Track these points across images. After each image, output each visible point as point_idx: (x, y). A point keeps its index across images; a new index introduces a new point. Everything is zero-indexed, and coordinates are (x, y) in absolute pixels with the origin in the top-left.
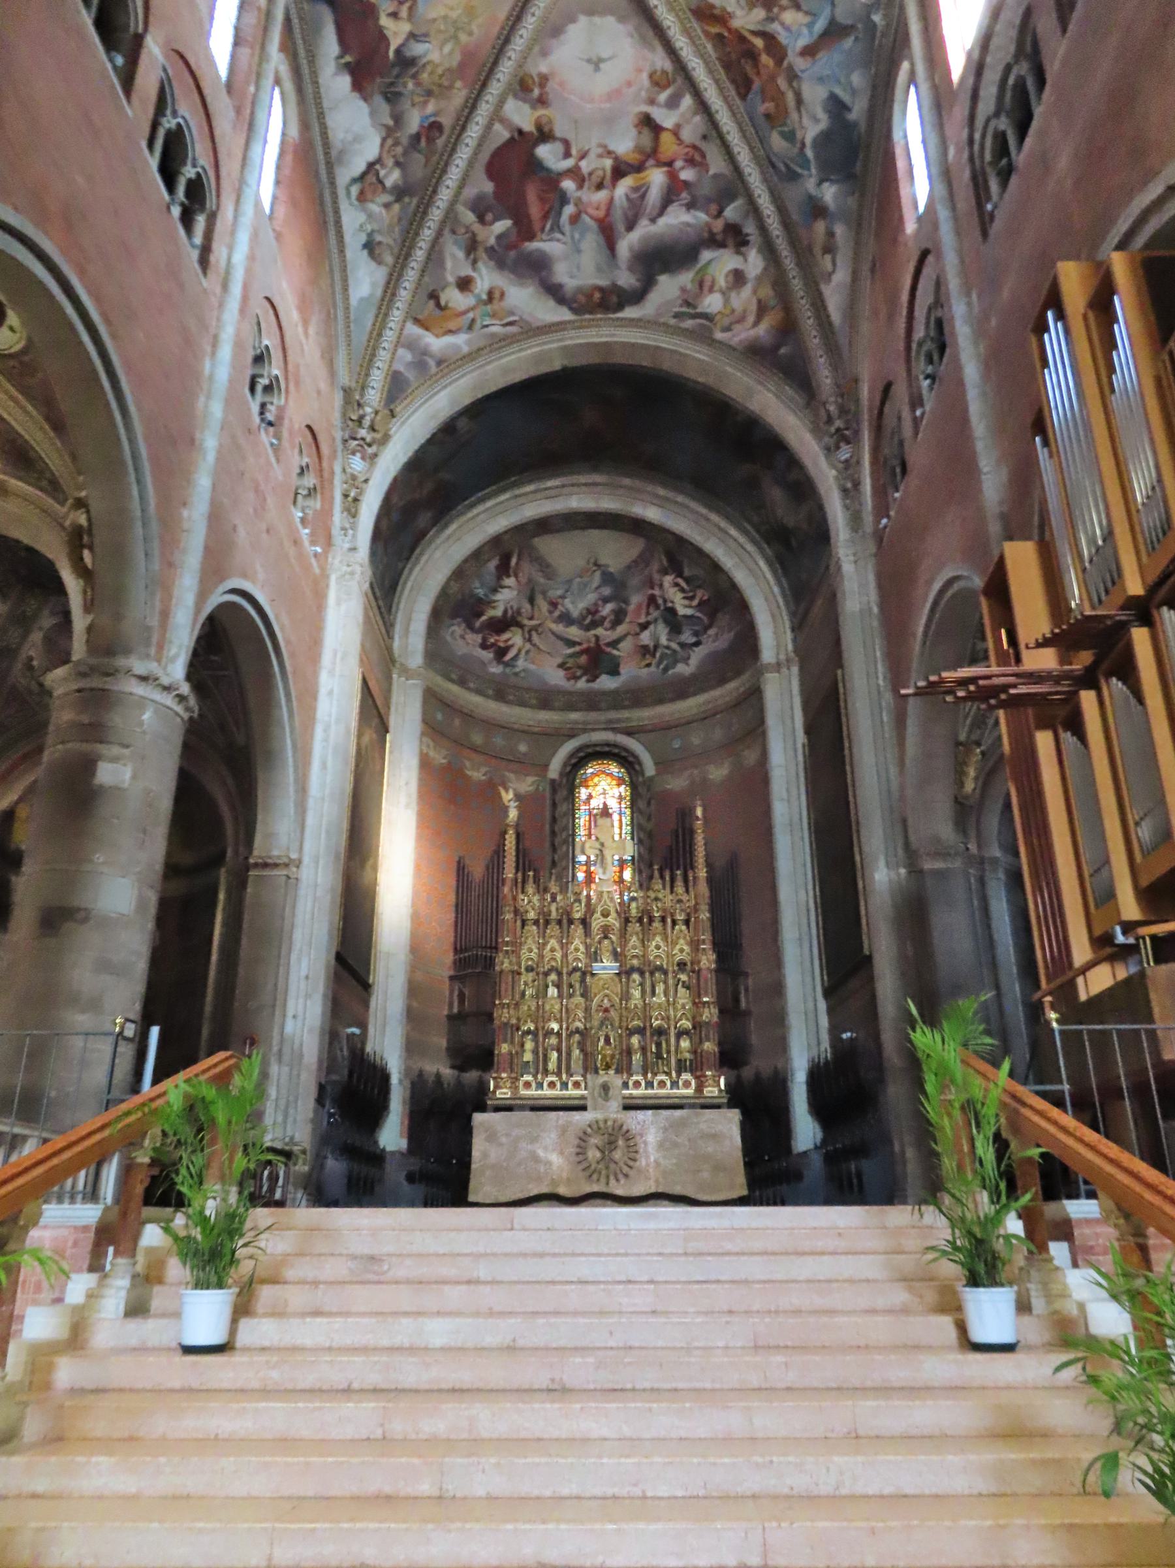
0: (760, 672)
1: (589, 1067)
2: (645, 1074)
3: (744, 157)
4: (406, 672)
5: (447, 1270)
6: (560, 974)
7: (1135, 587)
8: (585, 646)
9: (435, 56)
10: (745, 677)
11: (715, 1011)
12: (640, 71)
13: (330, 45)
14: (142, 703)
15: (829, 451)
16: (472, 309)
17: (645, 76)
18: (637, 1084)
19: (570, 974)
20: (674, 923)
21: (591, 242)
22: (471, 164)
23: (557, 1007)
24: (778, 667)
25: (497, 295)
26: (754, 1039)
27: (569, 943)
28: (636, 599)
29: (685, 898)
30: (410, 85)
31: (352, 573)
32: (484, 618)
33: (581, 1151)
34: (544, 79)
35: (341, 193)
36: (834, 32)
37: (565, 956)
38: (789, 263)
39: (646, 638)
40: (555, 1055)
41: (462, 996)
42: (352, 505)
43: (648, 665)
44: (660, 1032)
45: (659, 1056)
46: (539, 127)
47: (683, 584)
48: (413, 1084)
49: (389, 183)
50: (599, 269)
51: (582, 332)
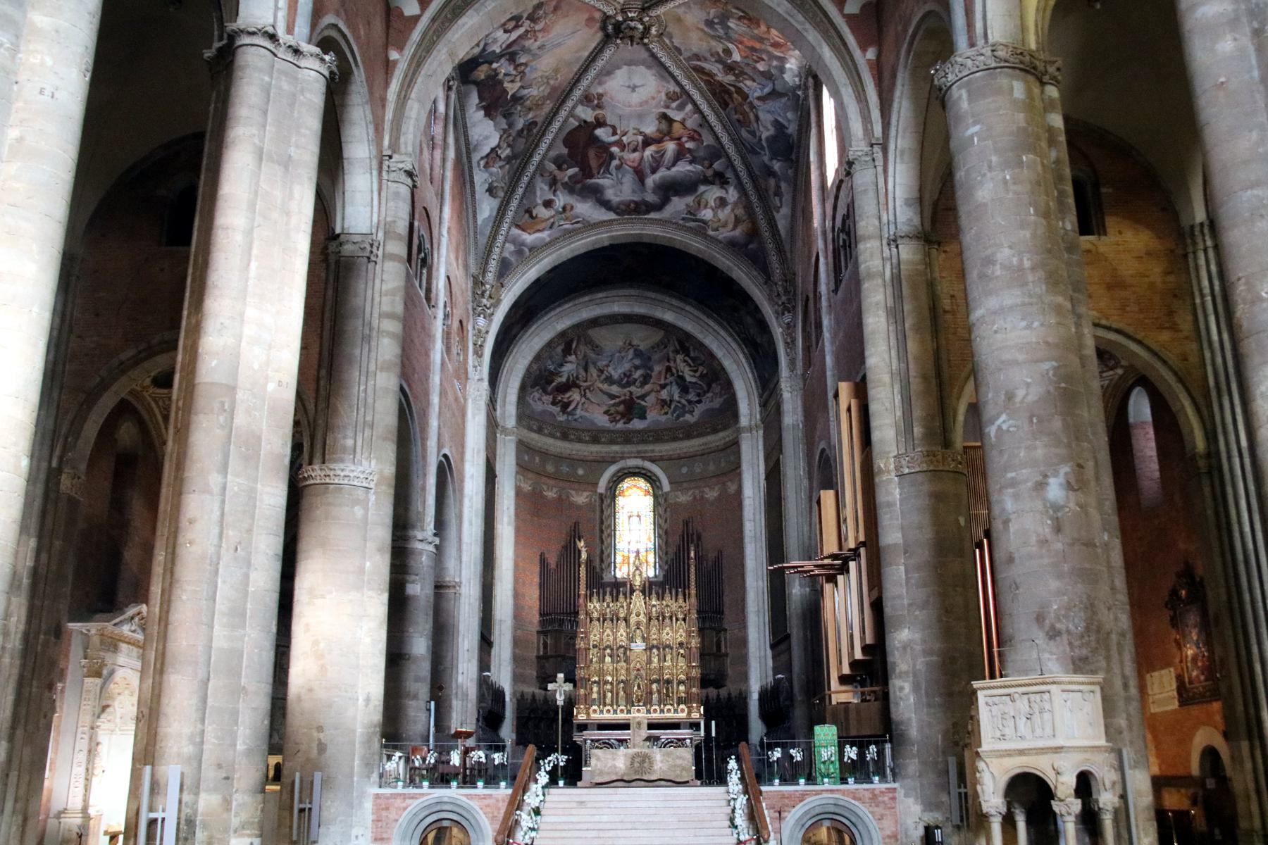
0: (739, 431)
1: (630, 702)
2: (659, 705)
3: (725, 139)
4: (505, 431)
5: (602, 805)
6: (612, 649)
7: (852, 544)
8: (623, 398)
11: (699, 671)
12: (660, 92)
13: (474, 99)
14: (421, 553)
15: (779, 315)
16: (553, 217)
18: (655, 711)
19: (618, 649)
20: (677, 620)
21: (628, 181)
22: (554, 140)
23: (611, 668)
24: (750, 429)
25: (568, 208)
26: (730, 671)
28: (657, 368)
29: (684, 605)
30: (519, 108)
31: (480, 396)
33: (632, 763)
34: (600, 96)
35: (474, 164)
36: (774, 94)
37: (615, 639)
38: (754, 198)
39: (664, 394)
40: (609, 695)
42: (478, 353)
43: (666, 413)
44: (668, 682)
45: (668, 695)
46: (596, 118)
47: (690, 361)
48: (518, 700)
50: (634, 191)
51: (622, 227)
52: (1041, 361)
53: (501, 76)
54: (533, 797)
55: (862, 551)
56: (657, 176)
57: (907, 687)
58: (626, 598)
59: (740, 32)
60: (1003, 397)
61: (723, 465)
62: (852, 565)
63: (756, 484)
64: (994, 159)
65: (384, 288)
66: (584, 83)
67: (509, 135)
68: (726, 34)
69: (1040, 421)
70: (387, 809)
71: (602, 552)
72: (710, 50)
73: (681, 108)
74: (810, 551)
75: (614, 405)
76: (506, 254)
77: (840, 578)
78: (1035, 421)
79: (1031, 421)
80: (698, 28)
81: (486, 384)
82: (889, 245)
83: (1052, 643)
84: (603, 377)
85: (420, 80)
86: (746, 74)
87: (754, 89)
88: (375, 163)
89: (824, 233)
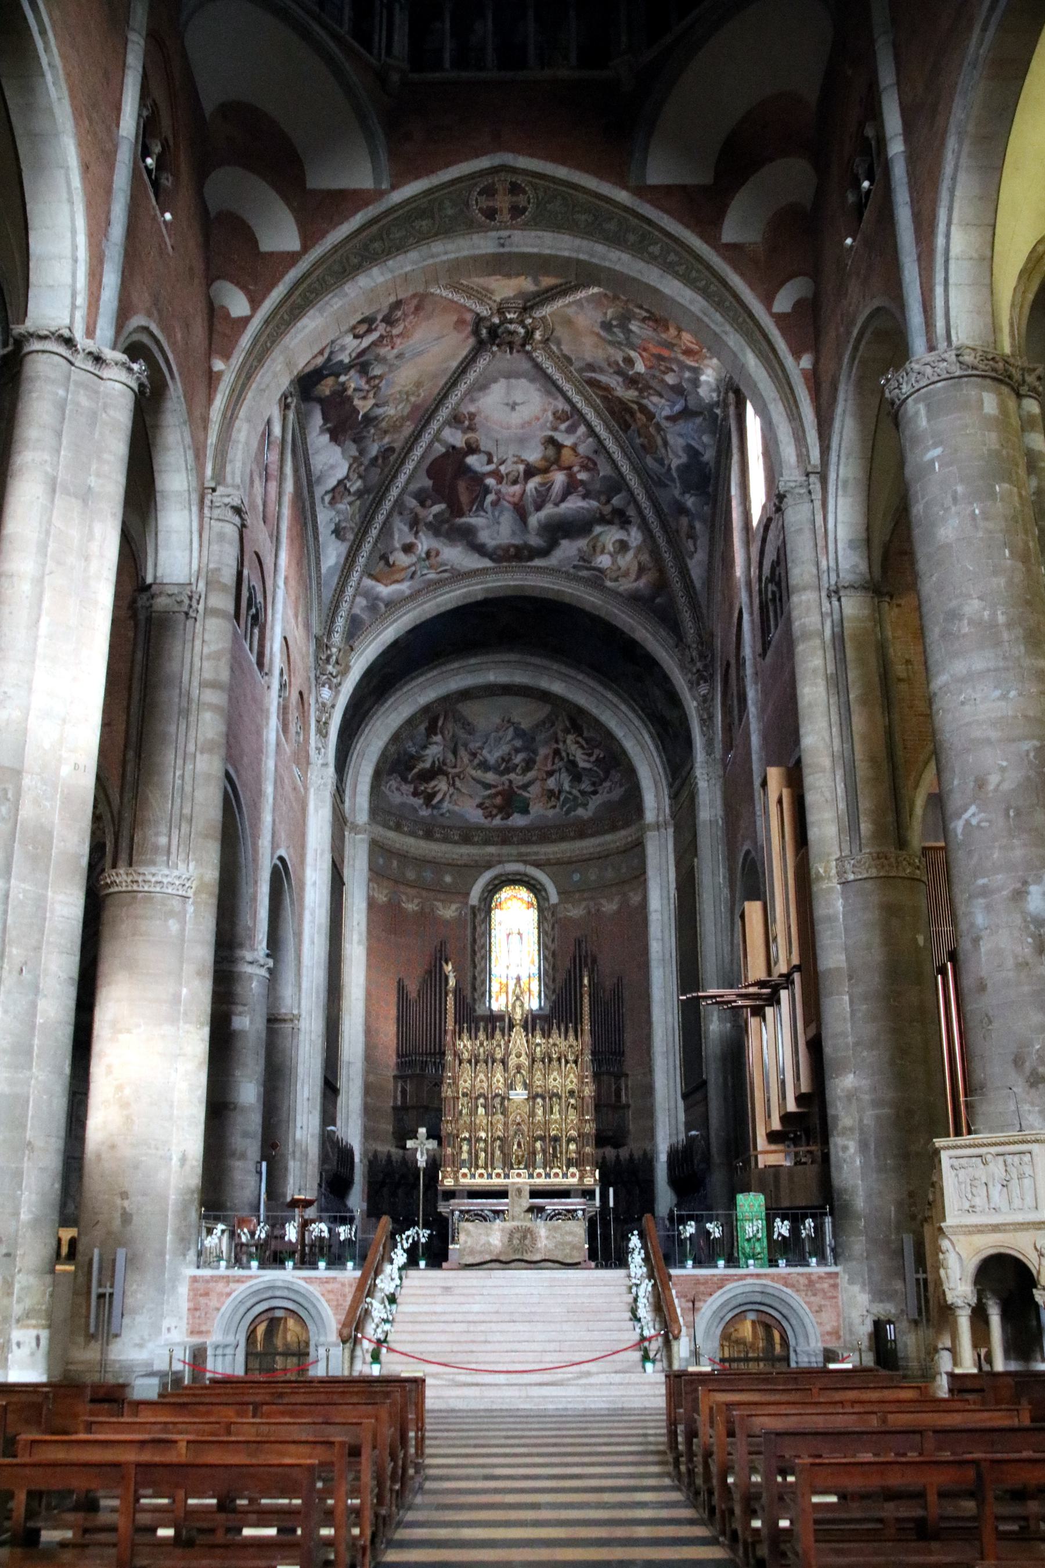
0: (643, 829)
2: (544, 1168)
3: (625, 468)
4: (355, 829)
5: (473, 1291)
6: (486, 1099)
7: (782, 968)
8: (500, 788)
9: (392, 412)
10: (631, 830)
11: (593, 1125)
12: (545, 410)
13: (317, 420)
14: (251, 977)
15: (693, 685)
16: (414, 564)
17: (550, 414)
18: (539, 1175)
19: (493, 1098)
20: (567, 1062)
22: (415, 469)
24: (658, 826)
25: (433, 553)
26: (631, 1127)
27: (493, 1076)
28: (543, 751)
29: (575, 1043)
30: (372, 431)
31: (325, 785)
32: (416, 770)
33: (510, 1240)
34: (472, 416)
35: (318, 501)
36: (686, 413)
37: (490, 1086)
38: (662, 542)
39: (551, 783)
40: (483, 1155)
41: (404, 1092)
42: (323, 732)
43: (554, 807)
44: (556, 1139)
45: (555, 1156)
46: (468, 443)
47: (583, 743)
48: (370, 1162)
49: (352, 490)
50: (514, 533)
52: (1019, 739)
53: (350, 392)
54: (386, 1284)
55: (797, 977)
56: (542, 514)
57: (852, 1146)
58: (503, 1035)
59: (644, 336)
60: (972, 784)
61: (624, 870)
62: (784, 994)
63: (665, 895)
64: (960, 489)
65: (206, 650)
66: (453, 400)
67: (361, 464)
68: (627, 339)
69: (1018, 814)
70: (206, 1294)
71: (474, 978)
72: (607, 359)
73: (572, 430)
74: (732, 977)
75: (489, 797)
76: (357, 611)
77: (769, 1011)
78: (1012, 814)
79: (1007, 815)
80: (593, 332)
81: (331, 770)
82: (829, 597)
83: (1033, 1090)
84: (476, 761)
85: (250, 395)
86: (651, 388)
87: (661, 407)
88: (195, 497)
89: (749, 584)
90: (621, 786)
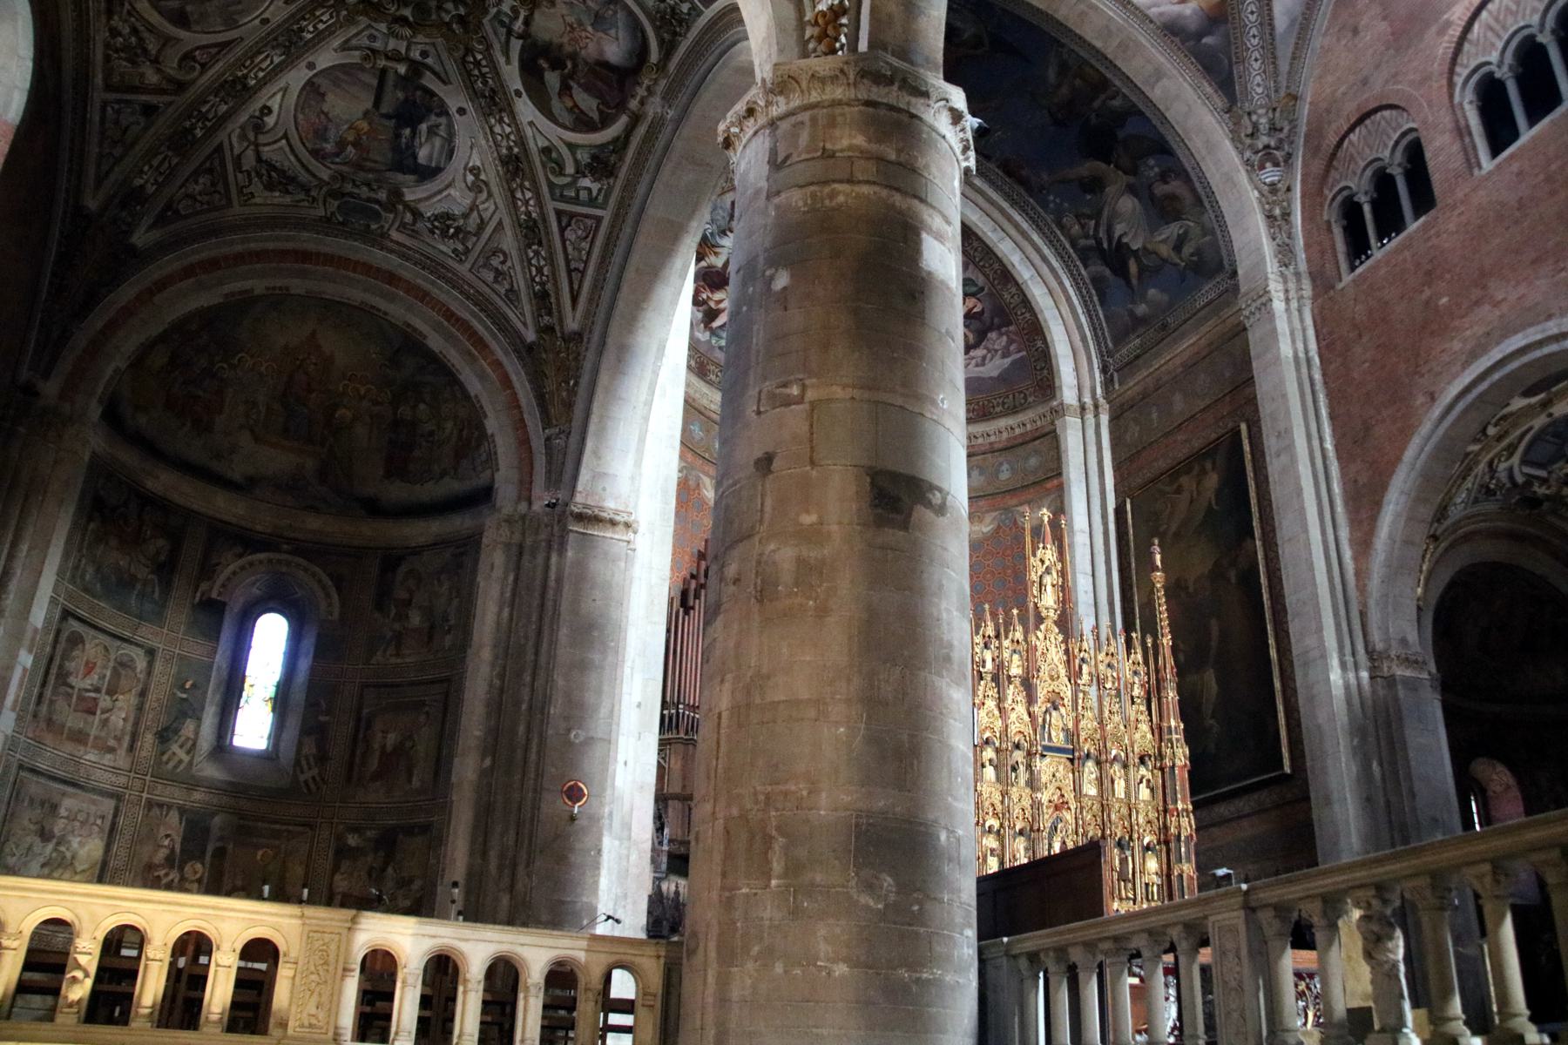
90: (1004, 356)
